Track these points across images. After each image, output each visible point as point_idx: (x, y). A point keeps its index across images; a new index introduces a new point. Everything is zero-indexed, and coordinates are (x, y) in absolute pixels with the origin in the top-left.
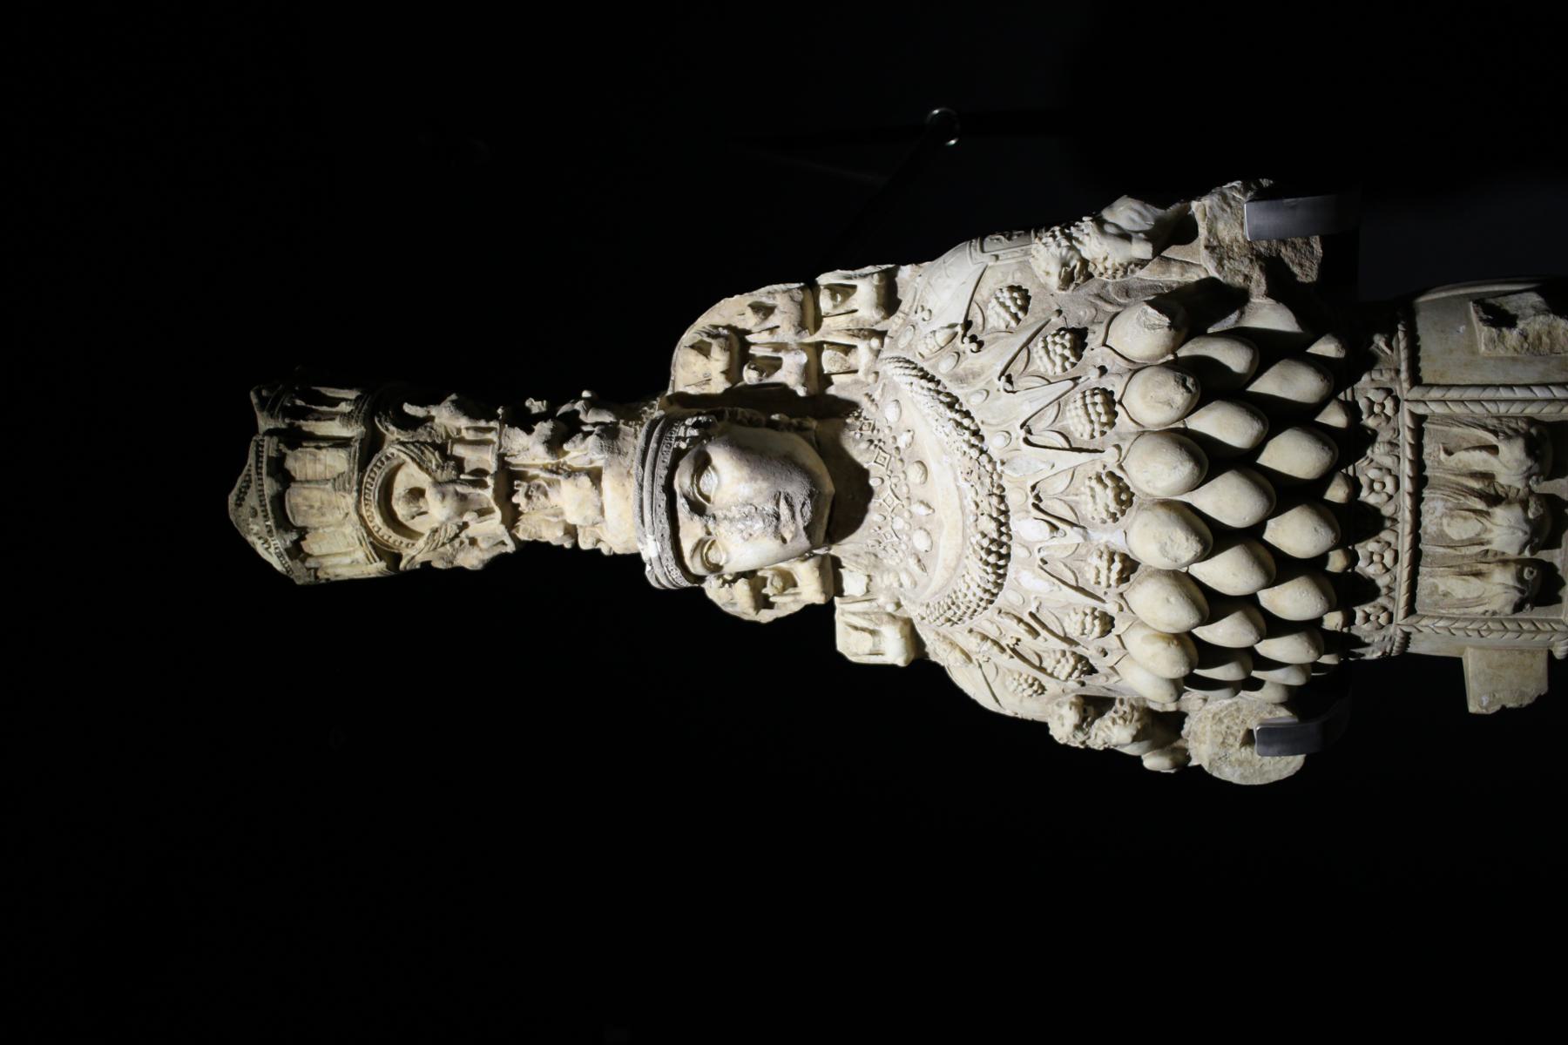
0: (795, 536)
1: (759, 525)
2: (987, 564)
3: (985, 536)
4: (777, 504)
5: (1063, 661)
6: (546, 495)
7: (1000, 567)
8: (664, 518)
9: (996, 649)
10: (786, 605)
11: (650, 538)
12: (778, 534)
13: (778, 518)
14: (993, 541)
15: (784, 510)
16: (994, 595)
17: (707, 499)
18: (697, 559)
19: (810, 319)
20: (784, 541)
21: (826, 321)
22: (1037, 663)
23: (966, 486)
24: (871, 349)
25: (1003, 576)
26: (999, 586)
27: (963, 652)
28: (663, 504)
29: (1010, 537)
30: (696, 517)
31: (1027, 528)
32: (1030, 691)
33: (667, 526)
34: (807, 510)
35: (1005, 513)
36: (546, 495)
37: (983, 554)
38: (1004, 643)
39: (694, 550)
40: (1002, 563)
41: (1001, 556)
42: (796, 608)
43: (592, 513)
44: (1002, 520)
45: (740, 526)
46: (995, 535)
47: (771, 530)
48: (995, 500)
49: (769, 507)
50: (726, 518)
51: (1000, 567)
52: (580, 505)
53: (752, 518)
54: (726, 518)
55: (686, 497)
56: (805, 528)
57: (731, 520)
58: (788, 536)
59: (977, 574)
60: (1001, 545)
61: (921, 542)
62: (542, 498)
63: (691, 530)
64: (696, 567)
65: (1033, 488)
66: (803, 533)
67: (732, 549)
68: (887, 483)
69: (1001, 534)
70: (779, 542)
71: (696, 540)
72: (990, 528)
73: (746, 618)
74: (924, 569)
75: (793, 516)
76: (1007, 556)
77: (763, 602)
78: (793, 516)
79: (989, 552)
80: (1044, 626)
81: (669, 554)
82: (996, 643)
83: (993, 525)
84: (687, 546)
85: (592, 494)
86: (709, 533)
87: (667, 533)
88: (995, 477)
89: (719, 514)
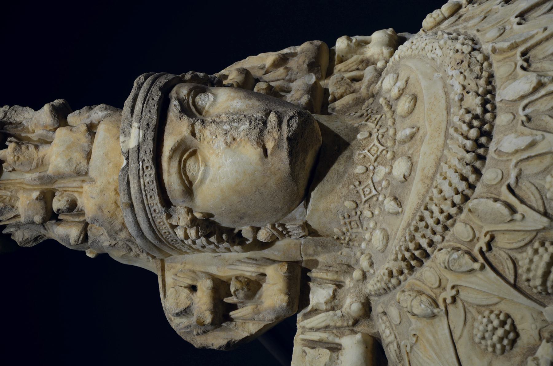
0: (277, 146)
1: (245, 126)
2: (467, 138)
3: (468, 111)
4: (267, 115)
5: (541, 250)
6: (37, 147)
7: (480, 146)
8: (154, 110)
9: (467, 256)
10: (247, 323)
11: (135, 124)
12: (261, 142)
13: (265, 123)
14: (476, 117)
15: (272, 118)
16: (472, 187)
17: (200, 114)
18: (175, 163)
19: (322, 65)
20: (265, 151)
21: (339, 67)
22: (512, 281)
23: (455, 73)
24: (376, 69)
25: (482, 158)
26: (478, 172)
27: (429, 296)
28: (156, 98)
29: (495, 117)
30: (185, 118)
31: (512, 88)
32: (500, 332)
33: (155, 117)
34: (294, 124)
35: (492, 92)
36: (37, 147)
37: (465, 127)
38: (476, 252)
39: (174, 150)
40: (483, 140)
41: (482, 133)
42: (253, 328)
43: (78, 156)
44: (488, 98)
45: (226, 127)
46: (479, 111)
47: (255, 132)
48: (482, 82)
49: (259, 115)
50: (214, 121)
51: (480, 146)
52: (69, 147)
53: (239, 120)
54: (214, 121)
55: (181, 101)
56: (288, 139)
57: (218, 123)
58: (270, 145)
59: (457, 154)
60: (484, 122)
61: (400, 168)
62: (32, 148)
63: (177, 129)
64: (171, 179)
65: (523, 54)
66: (285, 144)
67: (213, 160)
68: (374, 136)
69: (485, 111)
70: (260, 150)
71: (178, 138)
72: (474, 102)
73: (198, 341)
74: (400, 204)
75: (280, 124)
76: (489, 135)
77: (222, 313)
78: (280, 124)
79: (471, 126)
80: (522, 202)
81: (149, 145)
82: (469, 253)
83: (478, 100)
84: (169, 144)
85: (84, 140)
86: (193, 134)
87: (153, 124)
88: (485, 64)
89: (209, 119)
